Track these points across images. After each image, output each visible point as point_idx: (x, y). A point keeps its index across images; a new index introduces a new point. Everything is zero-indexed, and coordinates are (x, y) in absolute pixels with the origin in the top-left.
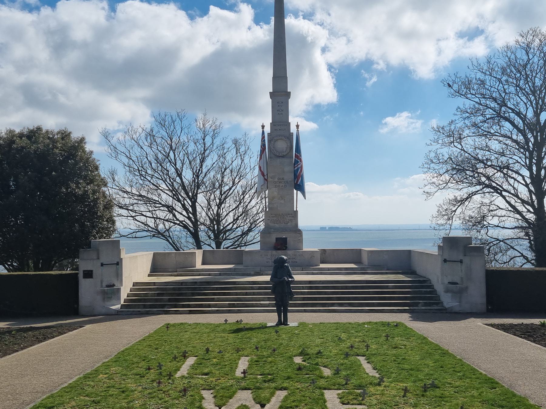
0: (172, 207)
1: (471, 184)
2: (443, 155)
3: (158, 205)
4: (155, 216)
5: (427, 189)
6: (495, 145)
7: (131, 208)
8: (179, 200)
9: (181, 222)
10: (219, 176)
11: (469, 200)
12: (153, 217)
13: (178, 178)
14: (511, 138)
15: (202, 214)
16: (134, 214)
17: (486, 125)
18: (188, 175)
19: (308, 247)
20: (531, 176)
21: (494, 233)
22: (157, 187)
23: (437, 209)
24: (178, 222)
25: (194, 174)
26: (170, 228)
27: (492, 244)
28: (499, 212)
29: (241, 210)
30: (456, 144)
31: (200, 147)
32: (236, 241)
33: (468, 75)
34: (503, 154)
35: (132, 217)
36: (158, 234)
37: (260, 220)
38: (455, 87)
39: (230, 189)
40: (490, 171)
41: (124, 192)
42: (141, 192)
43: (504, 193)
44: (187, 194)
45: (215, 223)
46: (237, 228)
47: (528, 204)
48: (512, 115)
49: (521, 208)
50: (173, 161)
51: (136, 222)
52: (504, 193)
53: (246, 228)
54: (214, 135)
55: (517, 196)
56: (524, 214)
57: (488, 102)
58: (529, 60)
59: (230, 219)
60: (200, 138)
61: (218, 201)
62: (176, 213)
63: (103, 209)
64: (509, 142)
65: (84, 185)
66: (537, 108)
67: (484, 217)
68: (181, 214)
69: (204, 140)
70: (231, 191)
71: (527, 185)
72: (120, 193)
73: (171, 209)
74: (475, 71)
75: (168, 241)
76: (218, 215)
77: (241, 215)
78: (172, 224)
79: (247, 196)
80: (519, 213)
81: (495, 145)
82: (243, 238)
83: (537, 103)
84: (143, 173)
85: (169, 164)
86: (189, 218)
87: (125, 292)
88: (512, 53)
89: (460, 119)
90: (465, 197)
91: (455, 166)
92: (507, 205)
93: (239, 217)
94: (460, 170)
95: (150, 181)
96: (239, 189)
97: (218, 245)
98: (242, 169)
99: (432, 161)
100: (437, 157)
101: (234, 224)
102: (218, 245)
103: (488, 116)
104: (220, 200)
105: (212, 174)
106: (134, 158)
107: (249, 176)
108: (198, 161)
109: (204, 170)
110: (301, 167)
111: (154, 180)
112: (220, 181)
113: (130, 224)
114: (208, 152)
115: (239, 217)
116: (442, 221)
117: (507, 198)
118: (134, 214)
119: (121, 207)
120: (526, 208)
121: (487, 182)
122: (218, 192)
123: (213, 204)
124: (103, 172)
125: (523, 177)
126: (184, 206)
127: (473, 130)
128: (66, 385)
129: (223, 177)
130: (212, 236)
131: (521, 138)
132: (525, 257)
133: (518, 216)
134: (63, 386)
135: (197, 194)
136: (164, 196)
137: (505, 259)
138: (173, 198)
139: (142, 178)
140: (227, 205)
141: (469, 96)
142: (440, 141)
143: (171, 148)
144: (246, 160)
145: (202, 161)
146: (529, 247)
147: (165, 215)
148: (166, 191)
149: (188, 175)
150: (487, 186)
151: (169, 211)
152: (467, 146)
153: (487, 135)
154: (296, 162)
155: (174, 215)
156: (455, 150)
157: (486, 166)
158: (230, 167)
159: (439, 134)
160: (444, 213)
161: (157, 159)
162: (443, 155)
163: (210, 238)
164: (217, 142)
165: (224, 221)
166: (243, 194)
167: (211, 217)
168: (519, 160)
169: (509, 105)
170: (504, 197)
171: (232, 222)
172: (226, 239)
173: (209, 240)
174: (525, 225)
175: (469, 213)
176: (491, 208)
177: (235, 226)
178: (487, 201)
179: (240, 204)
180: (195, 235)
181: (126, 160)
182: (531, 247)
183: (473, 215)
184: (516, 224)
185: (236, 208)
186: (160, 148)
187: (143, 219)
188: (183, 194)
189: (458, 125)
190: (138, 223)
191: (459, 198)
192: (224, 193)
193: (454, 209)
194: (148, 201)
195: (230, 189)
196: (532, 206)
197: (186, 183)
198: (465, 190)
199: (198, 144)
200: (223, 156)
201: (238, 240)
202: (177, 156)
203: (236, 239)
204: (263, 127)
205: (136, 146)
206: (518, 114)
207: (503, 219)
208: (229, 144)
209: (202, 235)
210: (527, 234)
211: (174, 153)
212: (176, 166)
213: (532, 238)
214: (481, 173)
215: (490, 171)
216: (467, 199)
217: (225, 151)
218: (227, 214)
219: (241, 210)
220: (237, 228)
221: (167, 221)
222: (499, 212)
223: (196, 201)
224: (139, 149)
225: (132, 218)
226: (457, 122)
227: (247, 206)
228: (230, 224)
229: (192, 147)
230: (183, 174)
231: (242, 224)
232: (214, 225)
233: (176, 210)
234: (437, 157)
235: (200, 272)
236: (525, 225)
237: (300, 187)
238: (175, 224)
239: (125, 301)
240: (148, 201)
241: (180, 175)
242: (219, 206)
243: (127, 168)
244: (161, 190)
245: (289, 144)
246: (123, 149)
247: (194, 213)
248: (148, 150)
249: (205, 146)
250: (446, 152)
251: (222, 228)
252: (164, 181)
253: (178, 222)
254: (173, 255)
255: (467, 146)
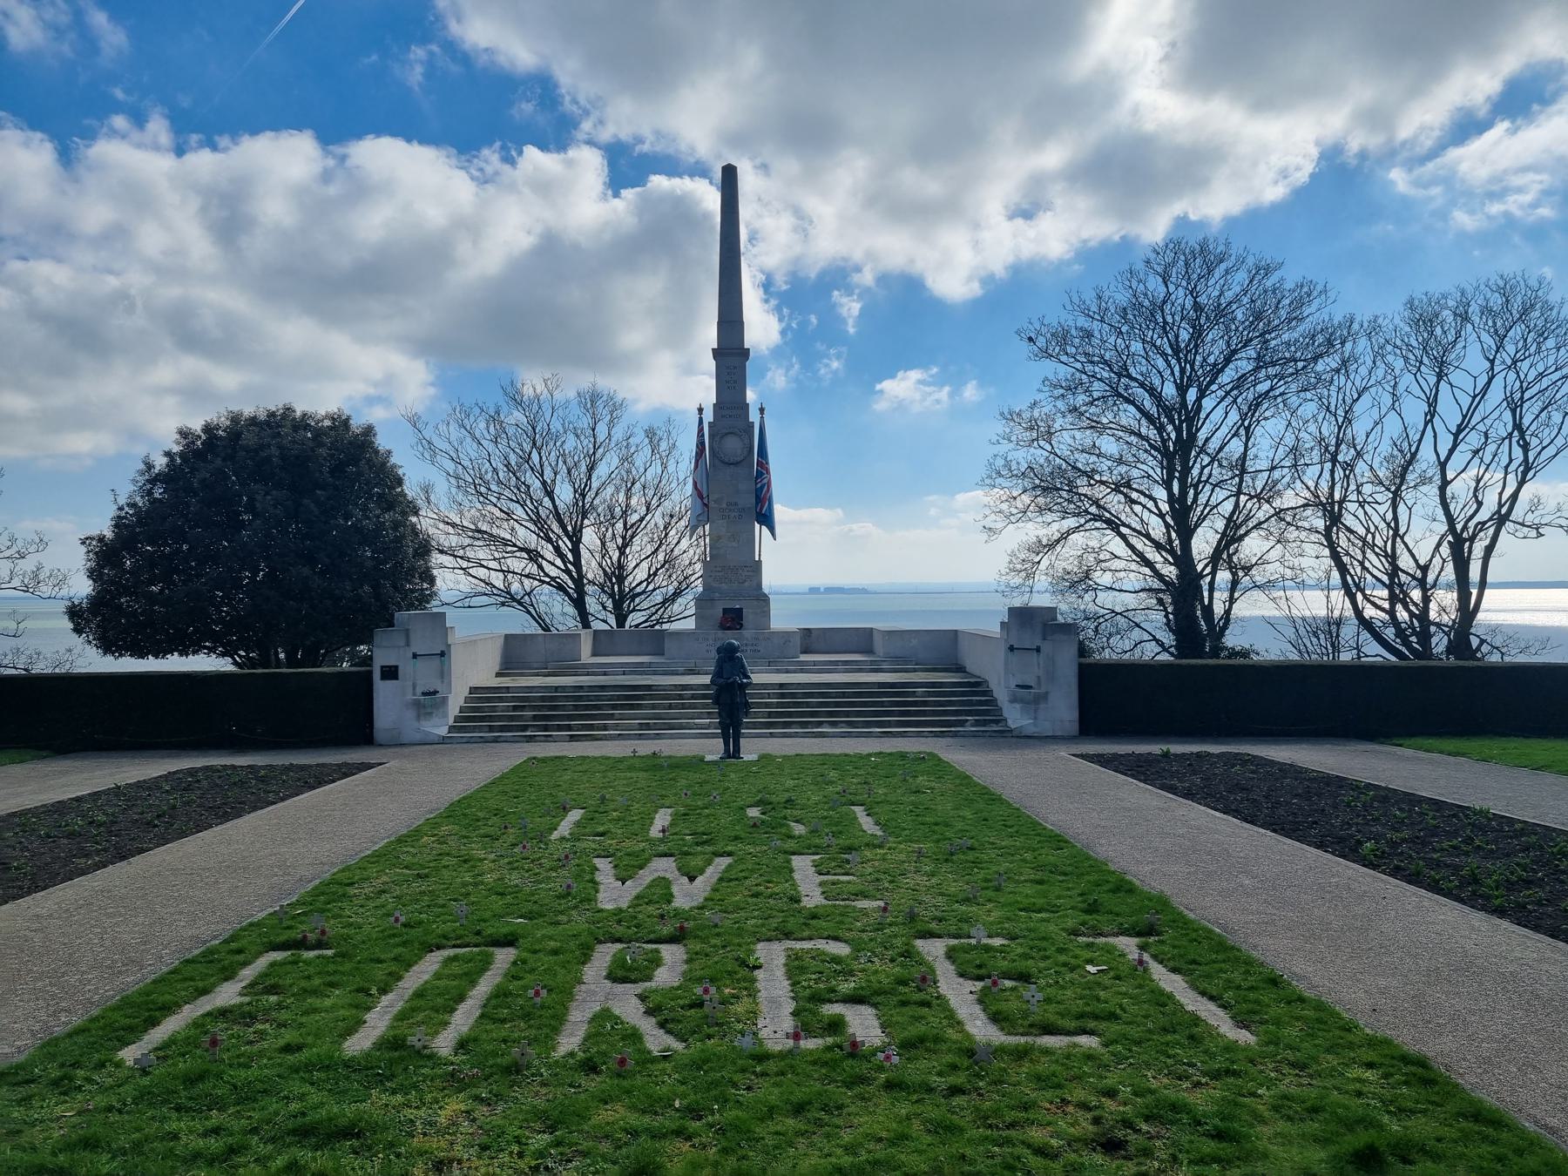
0: (536, 551)
1: (1065, 514)
2: (1018, 463)
3: (509, 549)
4: (504, 568)
5: (988, 523)
6: (1109, 445)
7: (461, 553)
8: (549, 540)
9: (553, 579)
10: (622, 497)
11: (1062, 542)
12: (502, 571)
13: (547, 499)
14: (1139, 435)
15: (591, 568)
16: (465, 564)
17: (1093, 409)
18: (564, 494)
19: (782, 619)
20: (1171, 499)
21: (1105, 599)
22: (509, 514)
23: (1008, 559)
24: (547, 580)
25: (575, 491)
26: (532, 591)
27: (1102, 620)
28: (1116, 564)
29: (661, 557)
30: (1042, 443)
31: (585, 443)
32: (653, 614)
33: (1062, 321)
34: (1120, 461)
35: (462, 569)
36: (510, 599)
37: (697, 576)
38: (1041, 342)
39: (642, 519)
40: (1100, 492)
41: (448, 523)
42: (479, 525)
43: (1123, 529)
44: (563, 526)
45: (614, 580)
46: (654, 590)
47: (1166, 550)
48: (1140, 392)
49: (1152, 554)
50: (538, 466)
51: (470, 578)
52: (1123, 529)
53: (671, 589)
54: (611, 421)
55: (1148, 536)
56: (1158, 566)
57: (1097, 369)
58: (1169, 294)
59: (641, 574)
60: (586, 426)
61: (620, 541)
62: (544, 563)
63: (413, 557)
64: (1133, 439)
65: (378, 512)
66: (1182, 379)
67: (1087, 576)
68: (553, 564)
69: (593, 430)
70: (644, 523)
71: (1161, 515)
72: (441, 526)
73: (534, 556)
74: (1076, 314)
75: (529, 612)
76: (621, 567)
77: (662, 566)
78: (536, 583)
79: (673, 533)
80: (1148, 563)
81: (1109, 445)
82: (666, 609)
83: (1183, 371)
84: (483, 490)
85: (529, 473)
86: (567, 572)
87: (456, 701)
88: (1140, 281)
89: (1049, 400)
90: (1055, 537)
91: (1037, 482)
92: (1130, 552)
93: (657, 570)
94: (1048, 488)
95: (496, 506)
96: (658, 518)
97: (621, 620)
98: (663, 482)
99: (999, 474)
100: (1008, 465)
101: (648, 584)
102: (621, 620)
103: (1096, 394)
104: (624, 538)
105: (610, 490)
106: (466, 463)
107: (676, 497)
108: (584, 469)
109: (595, 484)
110: (769, 483)
111: (504, 504)
112: (623, 505)
113: (458, 583)
114: (601, 451)
115: (657, 570)
116: (1017, 580)
117: (1130, 539)
118: (465, 564)
119: (442, 552)
120: (1162, 556)
121: (1093, 509)
122: (620, 526)
123: (611, 546)
124: (411, 489)
125: (1154, 500)
126: (557, 549)
127: (1069, 418)
128: (369, 852)
129: (628, 498)
130: (609, 604)
131: (1153, 433)
132: (1161, 644)
133: (1147, 571)
134: (363, 855)
135: (582, 527)
136: (521, 532)
137: (1127, 645)
138: (538, 535)
139: (481, 499)
140: (636, 548)
141: (1064, 358)
142: (1014, 438)
143: (534, 444)
144: (671, 468)
145: (591, 469)
146: (1166, 624)
147: (523, 565)
148: (524, 523)
149: (564, 494)
150: (1096, 518)
151: (531, 559)
152: (1061, 446)
153: (1096, 427)
154: (760, 474)
155: (540, 567)
156: (1039, 455)
157: (1092, 482)
158: (642, 479)
159: (1012, 424)
160: (1019, 567)
161: (508, 465)
162: (1018, 463)
163: (605, 608)
164: (618, 433)
165: (630, 578)
166: (665, 528)
167: (607, 569)
168: (1151, 472)
169: (1132, 371)
170: (1123, 537)
171: (646, 580)
172: (634, 610)
173: (603, 612)
174: (1156, 584)
175: (1061, 565)
176: (1102, 557)
177: (651, 587)
178: (1094, 544)
179: (659, 546)
180: (579, 603)
181: (450, 466)
182: (1168, 624)
183: (1069, 568)
184: (1143, 585)
185: (653, 553)
186: (513, 444)
187: (482, 573)
188: (555, 526)
189: (1045, 410)
190: (473, 580)
191: (1045, 542)
192: (632, 526)
193: (1037, 560)
194: (492, 539)
195: (642, 519)
196: (1172, 552)
197: (561, 507)
198: (1055, 526)
199: (582, 438)
200: (626, 459)
201: (657, 611)
202: (544, 459)
203: (653, 610)
204: (700, 410)
205: (469, 440)
206: (1152, 391)
207: (1122, 574)
208: (639, 437)
209: (592, 604)
210: (1160, 602)
211: (540, 454)
212: (542, 476)
213: (1170, 610)
214: (1085, 496)
215: (1100, 492)
216: (1058, 541)
217: (632, 451)
218: (637, 565)
219: (661, 557)
220: (654, 590)
221: (527, 576)
222: (1116, 564)
223: (579, 541)
224: (475, 445)
225: (462, 572)
226: (1043, 404)
227: (672, 551)
228: (641, 582)
229: (571, 443)
230: (556, 491)
231: (665, 583)
232: (613, 585)
233: (543, 558)
234: (1008, 465)
235: (587, 670)
236: (1156, 584)
237: (767, 520)
238: (544, 582)
239: (457, 719)
240: (492, 539)
241: (550, 494)
242: (621, 551)
243: (453, 480)
244: (516, 521)
245: (747, 441)
246: (445, 446)
247: (577, 563)
248: (491, 447)
249: (595, 442)
250: (1022, 457)
251: (627, 590)
252: (522, 505)
253: (547, 580)
254: (540, 639)
255: (1061, 446)
